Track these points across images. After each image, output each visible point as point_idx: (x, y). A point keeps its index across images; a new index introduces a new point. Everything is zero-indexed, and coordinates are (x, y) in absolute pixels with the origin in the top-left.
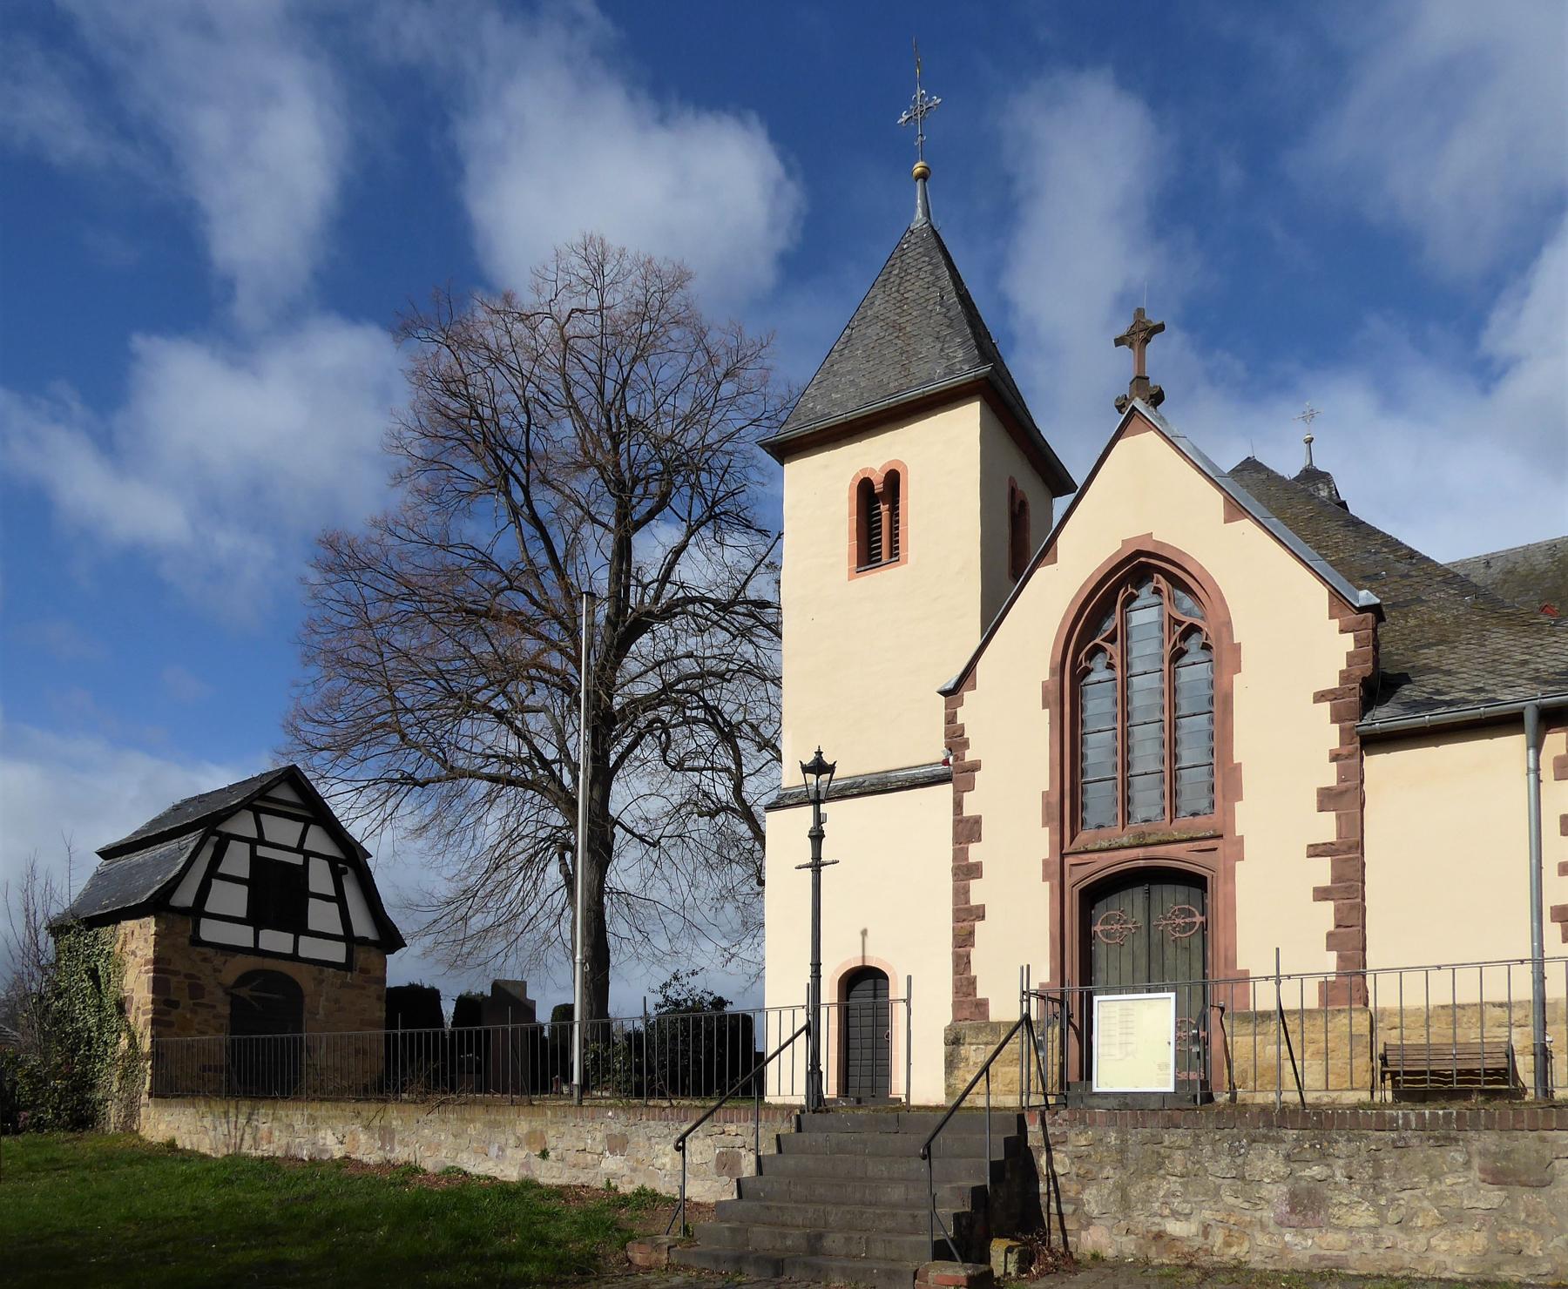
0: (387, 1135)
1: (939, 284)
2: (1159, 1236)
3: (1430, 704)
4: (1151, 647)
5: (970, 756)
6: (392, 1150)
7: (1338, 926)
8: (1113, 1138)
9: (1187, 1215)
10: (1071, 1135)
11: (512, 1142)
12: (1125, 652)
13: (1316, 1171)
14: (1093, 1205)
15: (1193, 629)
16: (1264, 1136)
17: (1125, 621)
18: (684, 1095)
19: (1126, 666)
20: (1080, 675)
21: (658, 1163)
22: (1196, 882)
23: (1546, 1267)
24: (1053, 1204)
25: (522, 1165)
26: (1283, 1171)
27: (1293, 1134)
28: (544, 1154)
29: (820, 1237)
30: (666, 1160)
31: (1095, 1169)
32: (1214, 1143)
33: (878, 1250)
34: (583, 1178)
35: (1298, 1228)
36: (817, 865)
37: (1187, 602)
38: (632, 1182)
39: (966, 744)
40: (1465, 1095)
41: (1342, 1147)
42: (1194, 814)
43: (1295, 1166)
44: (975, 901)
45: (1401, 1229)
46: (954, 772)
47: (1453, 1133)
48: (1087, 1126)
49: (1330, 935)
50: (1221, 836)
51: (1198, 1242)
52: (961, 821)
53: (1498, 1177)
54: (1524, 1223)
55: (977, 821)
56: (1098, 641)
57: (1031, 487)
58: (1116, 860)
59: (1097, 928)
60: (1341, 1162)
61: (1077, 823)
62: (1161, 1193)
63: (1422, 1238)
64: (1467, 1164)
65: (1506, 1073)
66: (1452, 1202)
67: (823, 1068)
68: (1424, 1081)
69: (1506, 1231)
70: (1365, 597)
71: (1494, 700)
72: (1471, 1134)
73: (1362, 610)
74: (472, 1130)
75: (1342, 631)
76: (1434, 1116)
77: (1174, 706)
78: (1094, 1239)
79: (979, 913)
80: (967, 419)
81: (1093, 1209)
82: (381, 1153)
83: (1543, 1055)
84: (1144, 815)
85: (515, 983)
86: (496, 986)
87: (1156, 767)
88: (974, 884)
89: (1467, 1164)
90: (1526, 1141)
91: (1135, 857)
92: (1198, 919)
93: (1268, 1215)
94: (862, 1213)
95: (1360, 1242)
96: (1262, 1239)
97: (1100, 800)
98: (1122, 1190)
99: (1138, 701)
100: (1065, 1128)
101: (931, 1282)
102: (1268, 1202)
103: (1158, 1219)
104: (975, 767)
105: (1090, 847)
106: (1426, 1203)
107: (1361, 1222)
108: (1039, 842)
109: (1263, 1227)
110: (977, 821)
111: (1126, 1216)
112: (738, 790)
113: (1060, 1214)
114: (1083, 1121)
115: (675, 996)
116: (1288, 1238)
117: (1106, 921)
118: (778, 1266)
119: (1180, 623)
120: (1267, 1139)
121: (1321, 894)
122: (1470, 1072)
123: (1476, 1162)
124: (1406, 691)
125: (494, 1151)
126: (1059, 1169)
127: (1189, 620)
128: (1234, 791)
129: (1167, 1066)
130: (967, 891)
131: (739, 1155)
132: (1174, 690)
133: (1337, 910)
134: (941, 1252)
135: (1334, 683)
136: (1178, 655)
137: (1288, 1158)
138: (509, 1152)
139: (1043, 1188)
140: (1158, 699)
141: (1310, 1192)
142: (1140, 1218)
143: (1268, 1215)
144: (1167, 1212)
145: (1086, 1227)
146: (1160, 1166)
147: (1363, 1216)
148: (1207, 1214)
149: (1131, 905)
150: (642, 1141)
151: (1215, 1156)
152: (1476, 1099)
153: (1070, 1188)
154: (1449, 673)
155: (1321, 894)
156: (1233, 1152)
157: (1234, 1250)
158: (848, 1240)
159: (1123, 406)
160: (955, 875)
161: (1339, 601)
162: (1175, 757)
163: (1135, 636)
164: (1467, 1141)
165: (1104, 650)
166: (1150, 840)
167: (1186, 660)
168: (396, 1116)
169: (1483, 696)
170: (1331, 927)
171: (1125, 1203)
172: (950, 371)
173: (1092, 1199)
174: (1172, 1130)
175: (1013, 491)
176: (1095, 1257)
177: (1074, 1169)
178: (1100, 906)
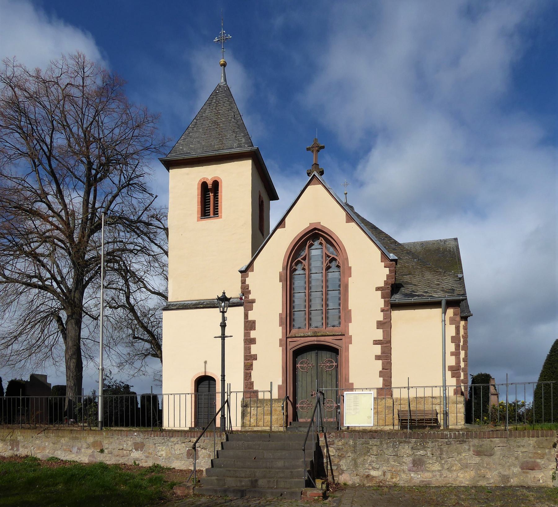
0: (15, 443)
1: (233, 110)
2: (368, 476)
3: (411, 295)
4: (319, 264)
5: (251, 297)
6: (18, 450)
7: (383, 369)
8: (351, 442)
9: (398, 468)
10: (336, 441)
11: (85, 446)
12: (309, 265)
13: (422, 452)
14: (344, 466)
15: (334, 259)
16: (404, 441)
17: (309, 253)
18: (122, 425)
19: (310, 270)
20: (293, 271)
21: (159, 454)
22: (335, 351)
23: (492, 481)
24: (329, 466)
25: (90, 456)
26: (411, 453)
27: (414, 440)
28: (102, 451)
29: (256, 481)
30: (163, 453)
31: (344, 453)
32: (387, 444)
33: (282, 485)
34: (122, 461)
35: (415, 472)
36: (223, 337)
37: (332, 249)
38: (146, 462)
39: (249, 292)
40: (424, 427)
41: (430, 444)
42: (333, 326)
43: (415, 451)
44: (253, 353)
45: (448, 471)
46: (245, 301)
47: (465, 439)
48: (342, 438)
49: (380, 372)
51: (382, 478)
52: (247, 322)
53: (478, 453)
54: (486, 467)
55: (254, 322)
56: (299, 259)
57: (265, 197)
58: (307, 341)
59: (298, 365)
60: (430, 449)
61: (291, 326)
62: (369, 461)
63: (455, 473)
64: (469, 450)
65: (436, 420)
66: (464, 462)
67: (226, 416)
68: (423, 423)
69: (481, 470)
70: (392, 256)
71: (432, 296)
72: (470, 440)
73: (392, 260)
74: (63, 441)
76: (434, 433)
77: (327, 287)
78: (344, 478)
79: (255, 357)
80: (246, 166)
81: (344, 467)
82: (12, 451)
83: (446, 414)
84: (316, 325)
85: (42, 375)
86: (33, 377)
87: (319, 307)
88: (253, 346)
89: (469, 450)
90: (487, 442)
91: (313, 340)
92: (335, 364)
93: (405, 468)
94: (270, 472)
95: (436, 475)
96: (404, 476)
97: (300, 318)
98: (355, 460)
99: (313, 283)
100: (333, 439)
101: (308, 495)
102: (405, 463)
103: (367, 470)
105: (297, 335)
106: (456, 462)
107: (436, 469)
108: (278, 332)
109: (404, 472)
110: (254, 322)
111: (356, 470)
112: (128, 298)
113: (332, 470)
114: (340, 436)
115: (108, 384)
116: (412, 475)
117: (302, 363)
118: (242, 493)
119: (329, 257)
120: (405, 442)
121: (378, 358)
122: (421, 420)
123: (472, 449)
124: (402, 289)
125: (75, 450)
126: (331, 454)
127: (332, 256)
128: (349, 319)
129: (371, 417)
130: (250, 349)
132: (327, 281)
133: (383, 363)
134: (309, 484)
136: (328, 268)
137: (412, 448)
138: (83, 450)
139: (325, 460)
140: (321, 283)
141: (419, 459)
142: (361, 471)
143: (405, 468)
144: (371, 468)
145: (341, 474)
146: (368, 452)
147: (437, 467)
148: (385, 468)
149: (311, 357)
150: (151, 445)
151: (387, 448)
152: (428, 429)
153: (335, 460)
154: (415, 285)
155: (378, 358)
156: (394, 447)
157: (394, 480)
158: (269, 482)
159: (310, 173)
160: (245, 342)
161: (384, 257)
162: (327, 305)
163: (312, 260)
164: (469, 442)
165: (302, 263)
166: (319, 334)
167: (330, 270)
168: (19, 436)
169: (428, 294)
170: (381, 369)
171: (356, 465)
172: (240, 146)
173: (344, 464)
174: (373, 439)
175: (260, 196)
176: (345, 484)
177: (337, 454)
178: (299, 357)
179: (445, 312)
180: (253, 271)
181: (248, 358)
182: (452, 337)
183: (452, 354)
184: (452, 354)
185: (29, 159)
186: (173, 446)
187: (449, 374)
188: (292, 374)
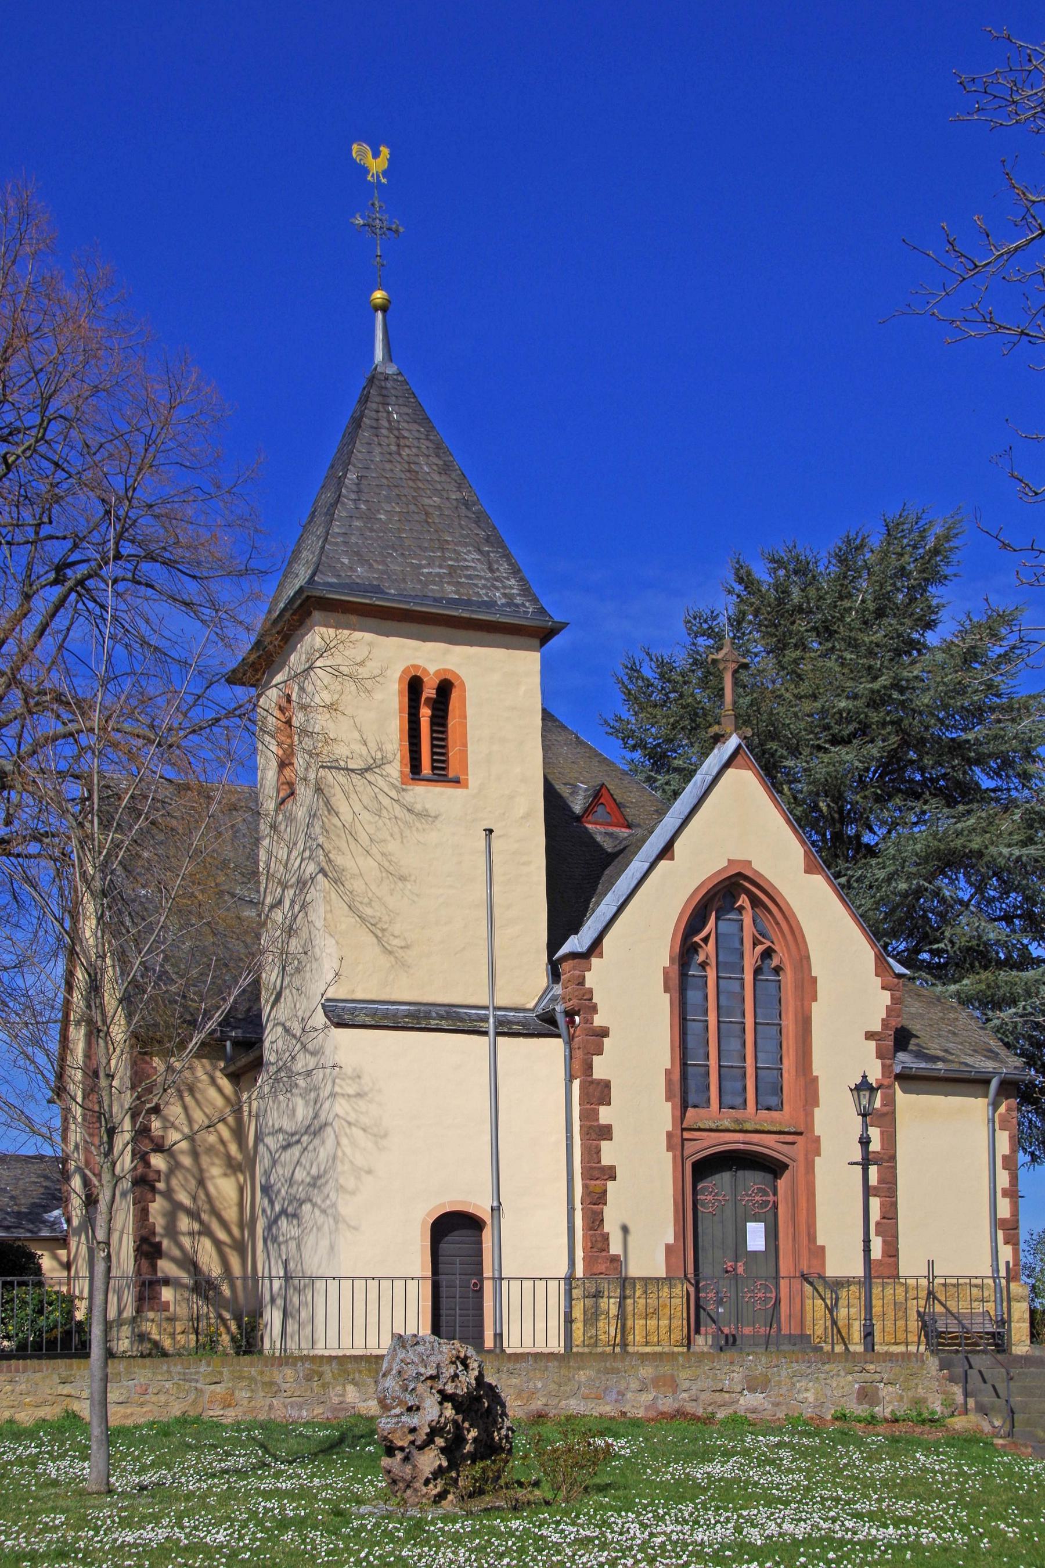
11: (635, 1385)
21: (800, 1397)
22: (774, 1168)
30: (808, 1395)
42: (768, 1109)
44: (605, 1161)
50: (801, 1134)
55: (606, 1085)
58: (722, 1140)
74: (582, 1376)
75: (883, 988)
79: (610, 1173)
91: (734, 1141)
104: (604, 1033)
108: (664, 1115)
110: (606, 1085)
130: (598, 1152)
131: (877, 1388)
135: (878, 1028)
138: (629, 1395)
149: (724, 1179)
166: (748, 1126)
179: (995, 1105)
180: (601, 955)
181: (596, 1174)
182: (1004, 1157)
183: (1005, 1193)
184: (1005, 1193)
185: (318, 635)
186: (828, 1381)
187: (1000, 1234)
188: (691, 1217)
